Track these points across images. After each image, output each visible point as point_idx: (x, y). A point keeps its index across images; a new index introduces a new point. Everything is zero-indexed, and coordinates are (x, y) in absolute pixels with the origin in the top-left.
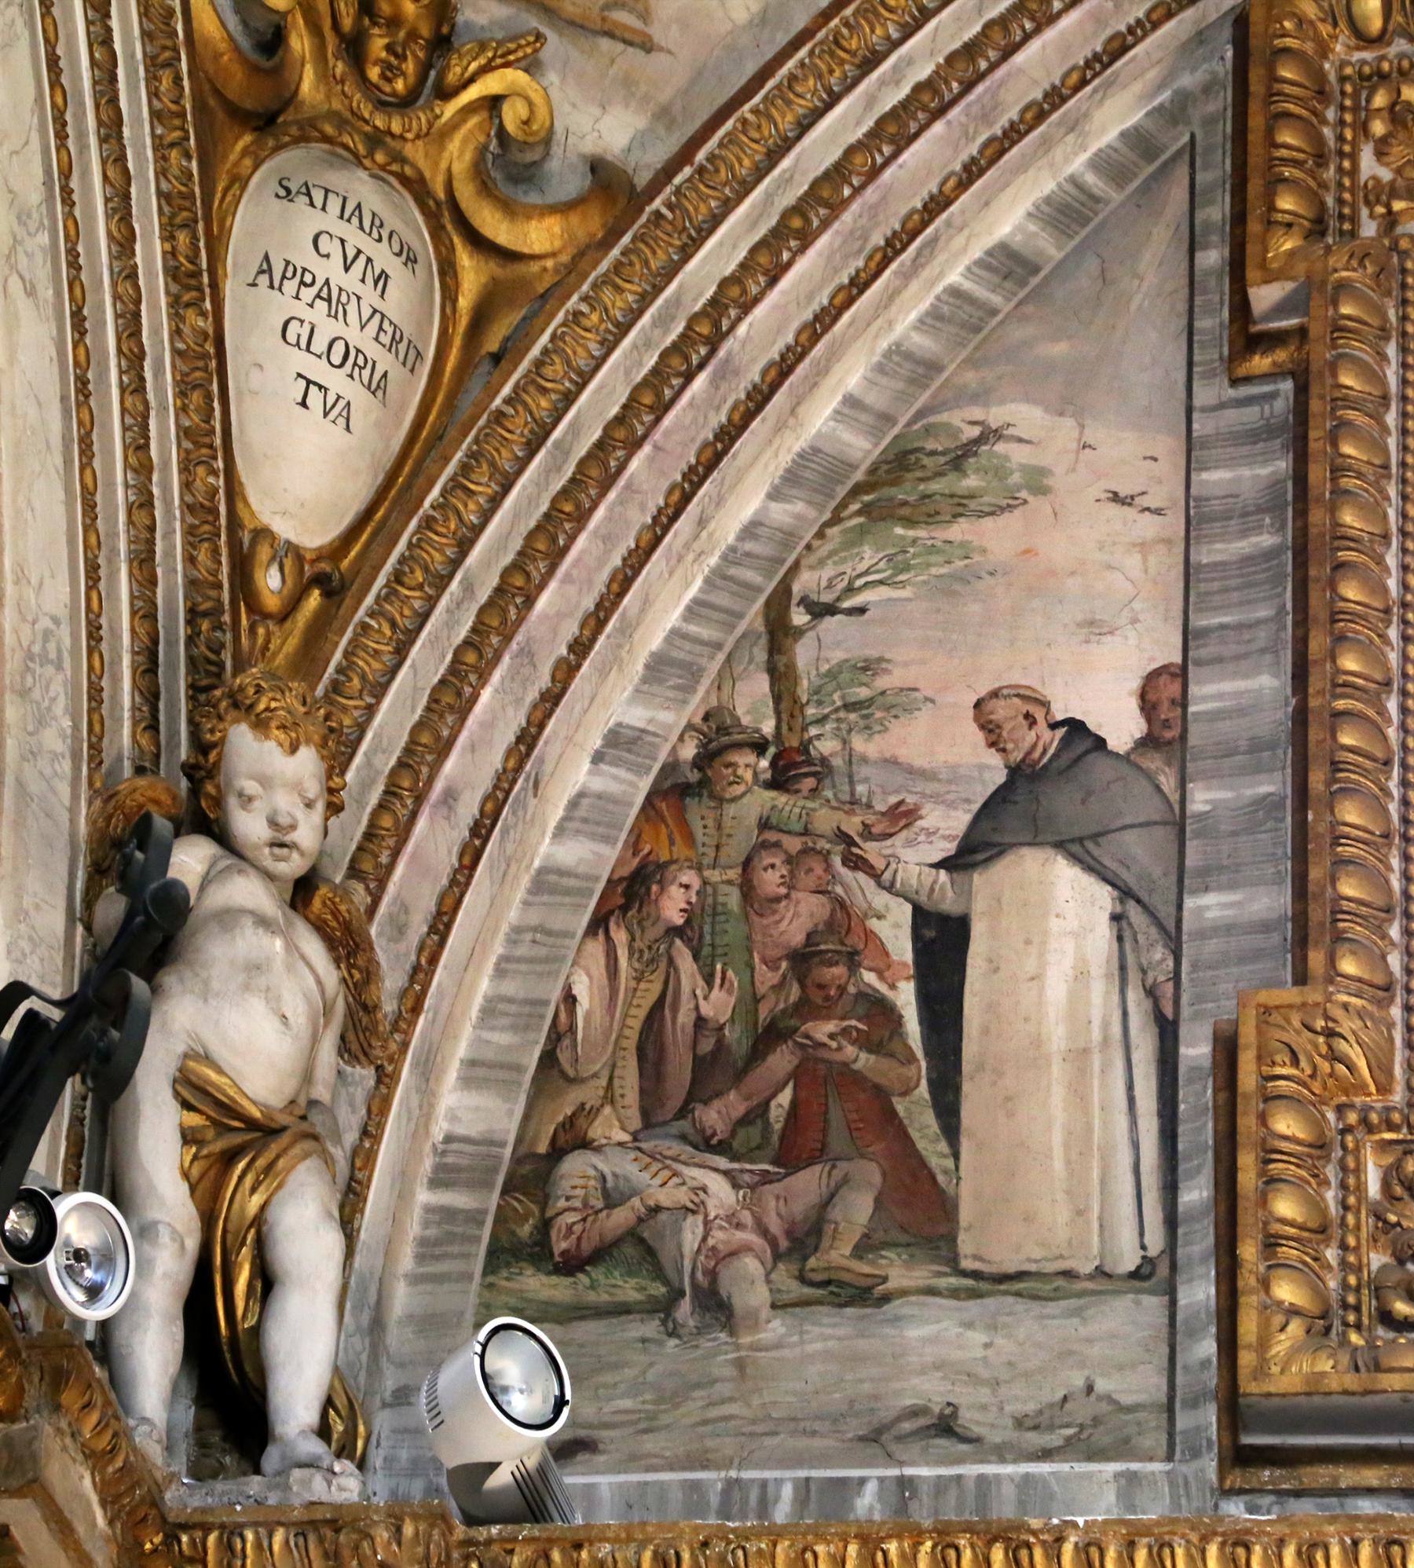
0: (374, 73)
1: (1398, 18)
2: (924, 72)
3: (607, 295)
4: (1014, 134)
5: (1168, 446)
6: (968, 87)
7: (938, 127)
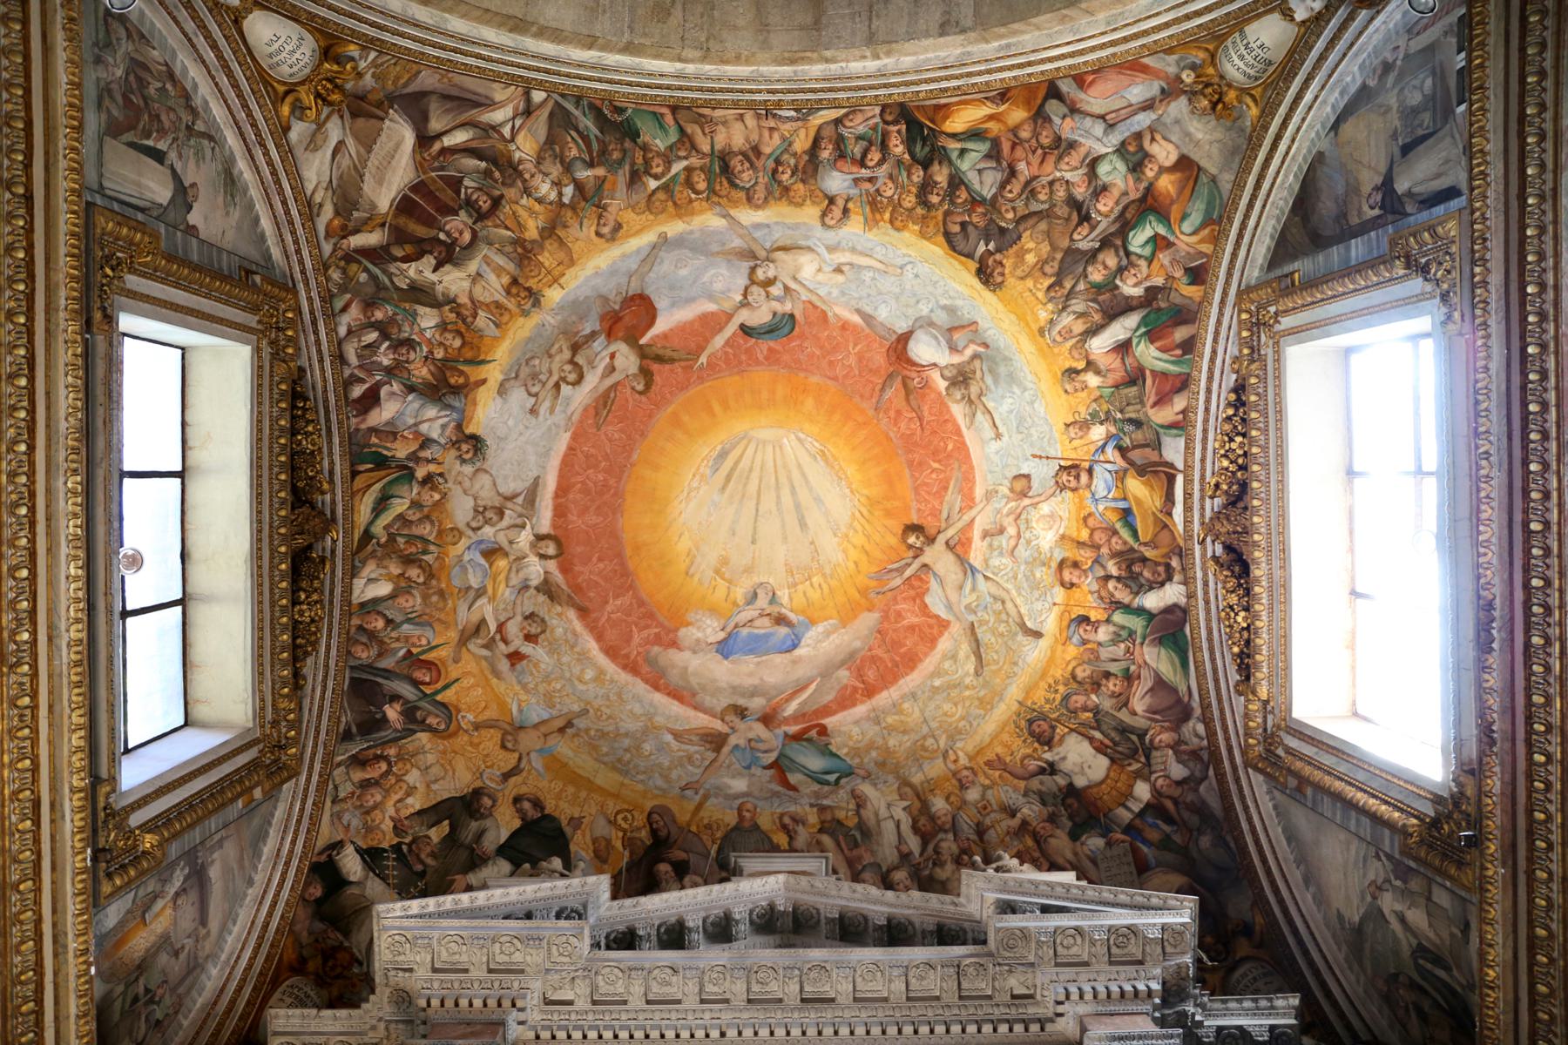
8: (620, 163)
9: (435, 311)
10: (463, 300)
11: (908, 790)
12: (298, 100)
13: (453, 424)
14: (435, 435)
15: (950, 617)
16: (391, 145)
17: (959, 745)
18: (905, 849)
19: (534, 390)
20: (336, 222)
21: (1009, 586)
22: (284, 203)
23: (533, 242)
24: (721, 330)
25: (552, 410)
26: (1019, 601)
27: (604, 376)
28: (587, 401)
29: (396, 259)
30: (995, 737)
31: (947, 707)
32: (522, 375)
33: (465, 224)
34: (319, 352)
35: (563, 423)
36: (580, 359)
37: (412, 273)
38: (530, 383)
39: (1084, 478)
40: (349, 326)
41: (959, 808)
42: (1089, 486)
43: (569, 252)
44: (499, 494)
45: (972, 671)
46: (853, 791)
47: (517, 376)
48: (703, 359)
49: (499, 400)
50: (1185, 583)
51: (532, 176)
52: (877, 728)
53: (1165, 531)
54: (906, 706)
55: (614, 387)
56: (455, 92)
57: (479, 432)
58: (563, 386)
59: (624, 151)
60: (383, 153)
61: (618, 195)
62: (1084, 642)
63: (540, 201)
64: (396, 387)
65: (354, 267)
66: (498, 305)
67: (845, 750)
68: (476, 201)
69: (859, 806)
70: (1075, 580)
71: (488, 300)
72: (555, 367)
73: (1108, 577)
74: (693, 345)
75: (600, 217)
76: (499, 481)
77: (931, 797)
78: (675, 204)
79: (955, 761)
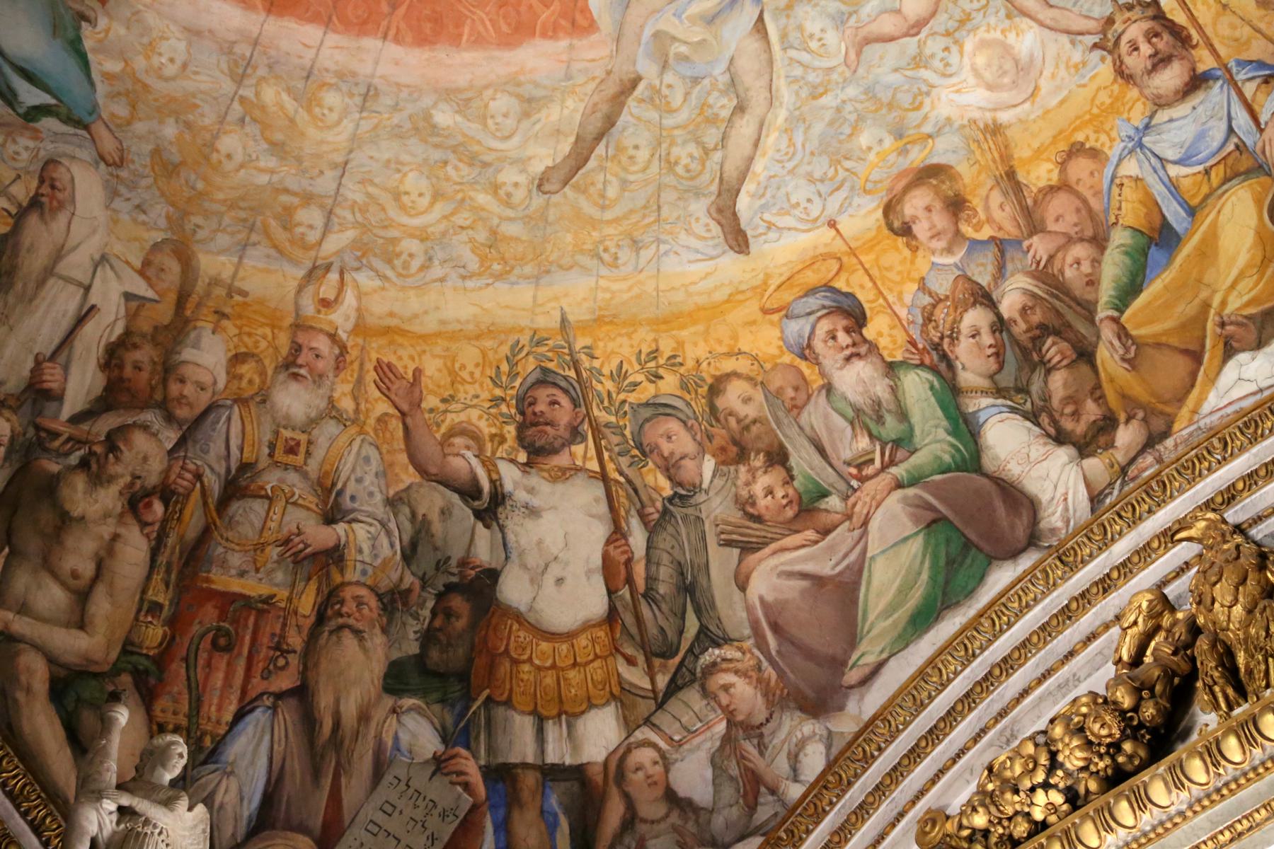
11: (174, 267)
15: (606, 22)
17: (365, 280)
18: (52, 378)
21: (786, 94)
26: (771, 140)
30: (451, 335)
31: (414, 183)
39: (1170, 78)
41: (241, 401)
42: (1160, 103)
45: (538, 167)
46: (51, 162)
50: (1096, 499)
52: (228, 86)
53: (1181, 365)
54: (332, 98)
62: (806, 351)
67: (114, 66)
69: (35, 203)
70: (920, 230)
73: (985, 298)
77: (206, 326)
79: (325, 304)
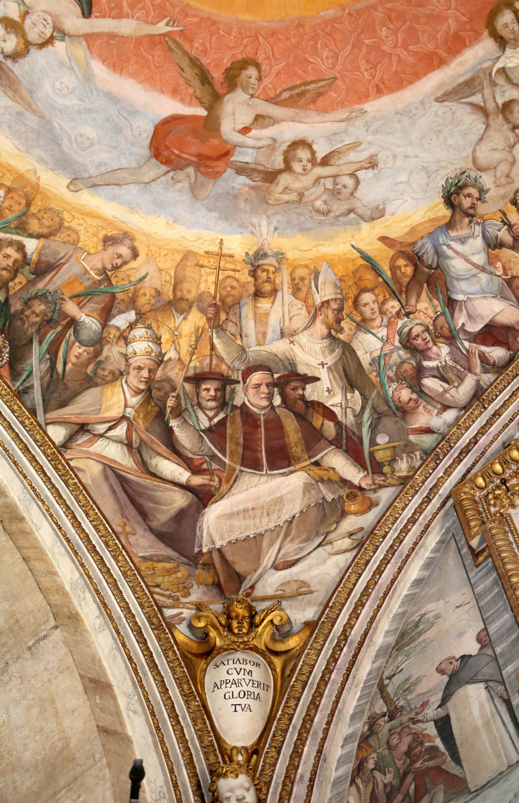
0: (236, 631)
1: (488, 480)
2: (382, 557)
3: (315, 645)
4: (408, 556)
5: (467, 590)
6: (393, 554)
7: (389, 566)
8: (42, 297)
9: (355, 345)
10: (320, 328)
12: (273, 639)
13: (453, 234)
14: (478, 242)
16: (236, 522)
19: (349, 182)
20: (353, 508)
22: (379, 571)
23: (203, 311)
24: (112, 36)
25: (356, 145)
27: (274, 121)
28: (313, 116)
29: (338, 424)
32: (345, 207)
33: (246, 391)
34: (489, 423)
35: (359, 123)
36: (278, 162)
37: (338, 398)
38: (346, 192)
40: (439, 413)
43: (180, 266)
44: (488, 126)
47: (351, 211)
48: (162, 28)
49: (389, 209)
51: (140, 368)
55: (275, 101)
56: (131, 511)
57: (439, 200)
58: (320, 155)
59: (27, 303)
60: (249, 522)
61: (77, 270)
63: (157, 340)
64: (461, 319)
65: (380, 456)
66: (296, 290)
68: (214, 399)
71: (300, 304)
72: (308, 180)
74: (157, 52)
75: (116, 268)
76: (474, 138)
78: (28, 205)
